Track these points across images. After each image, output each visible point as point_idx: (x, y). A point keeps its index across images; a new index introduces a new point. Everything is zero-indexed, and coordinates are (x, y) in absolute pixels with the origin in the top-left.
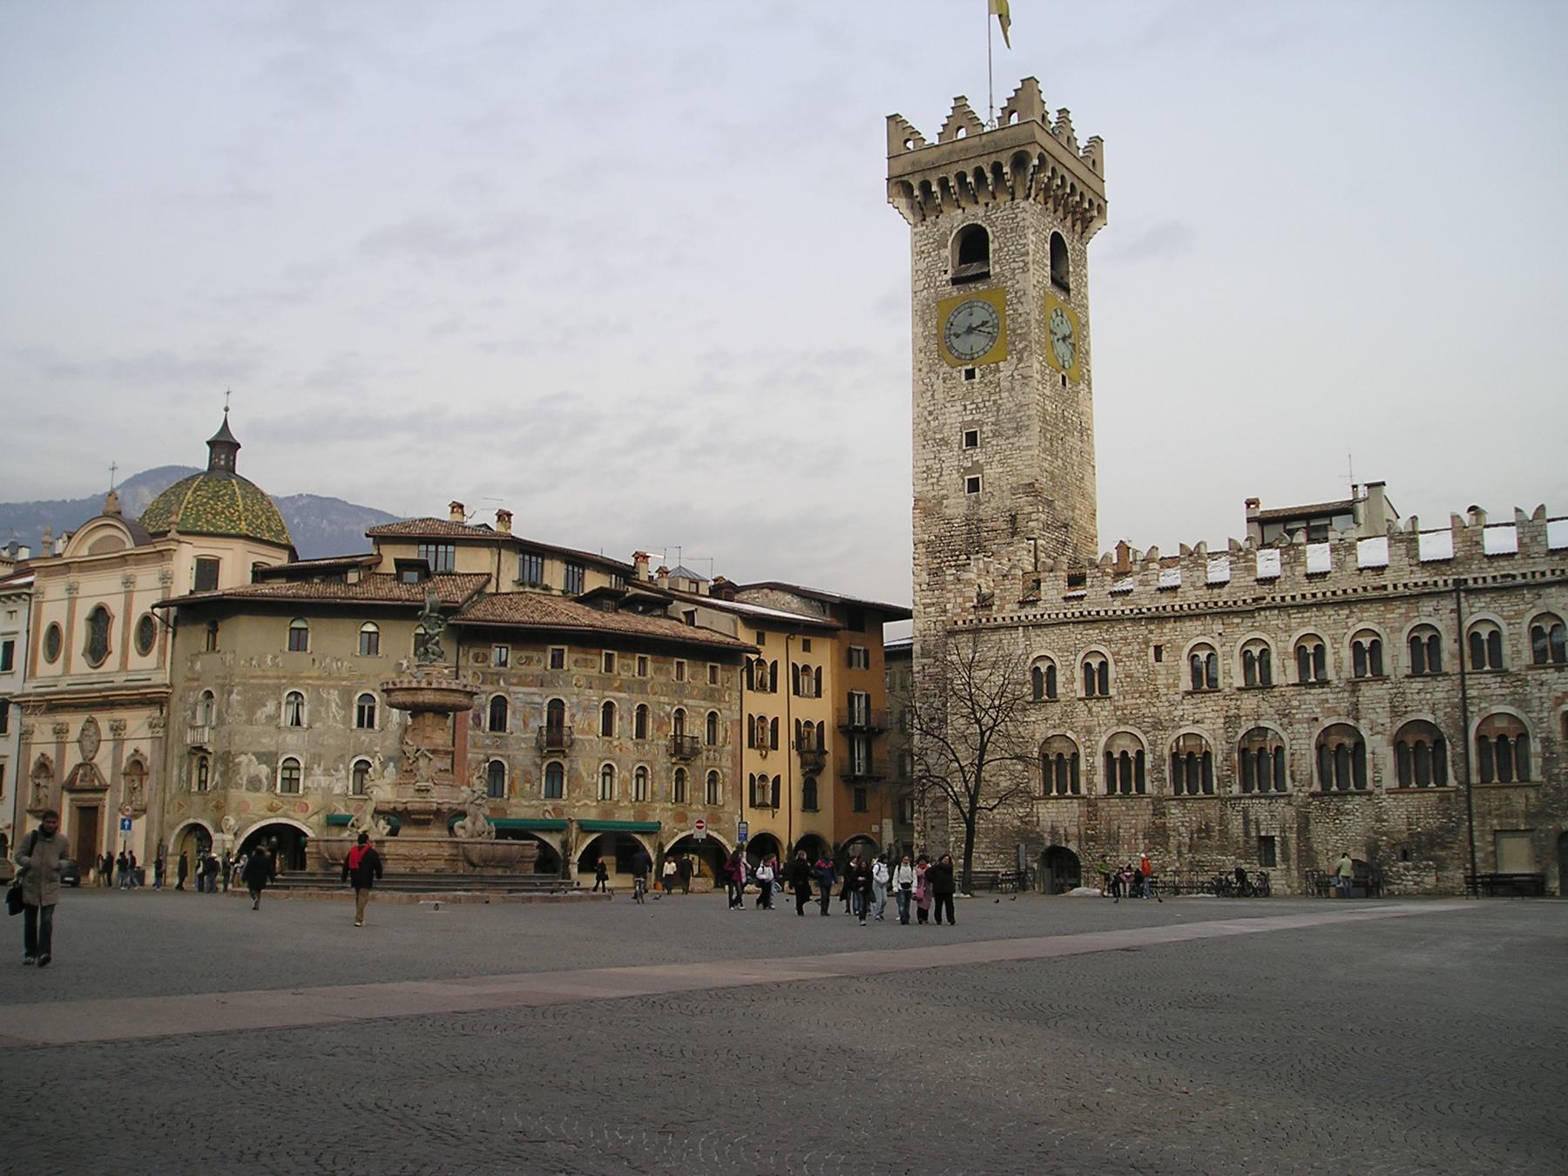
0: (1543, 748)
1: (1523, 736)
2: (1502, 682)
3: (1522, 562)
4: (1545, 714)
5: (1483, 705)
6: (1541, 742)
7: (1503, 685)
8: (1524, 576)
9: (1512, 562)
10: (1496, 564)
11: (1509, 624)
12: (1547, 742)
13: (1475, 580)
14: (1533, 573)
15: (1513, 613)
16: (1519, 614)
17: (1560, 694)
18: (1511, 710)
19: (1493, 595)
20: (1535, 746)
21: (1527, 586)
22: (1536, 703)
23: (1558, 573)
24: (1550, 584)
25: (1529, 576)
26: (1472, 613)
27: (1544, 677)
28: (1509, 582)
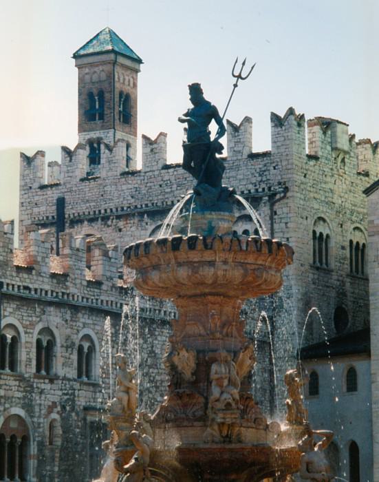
0: (38, 450)
1: (26, 439)
2: (19, 386)
3: (35, 278)
4: (42, 420)
5: (7, 406)
6: (38, 445)
7: (20, 388)
8: (36, 290)
9: (31, 276)
10: (21, 275)
11: (26, 333)
12: (41, 445)
13: (8, 285)
14: (41, 290)
15: (28, 323)
16: (32, 325)
17: (50, 404)
18: (22, 413)
19: (18, 303)
20: (33, 449)
21: (39, 301)
22: (37, 409)
23: (55, 294)
24: (50, 304)
25: (39, 291)
26: (5, 316)
27: (43, 386)
28: (25, 293)
